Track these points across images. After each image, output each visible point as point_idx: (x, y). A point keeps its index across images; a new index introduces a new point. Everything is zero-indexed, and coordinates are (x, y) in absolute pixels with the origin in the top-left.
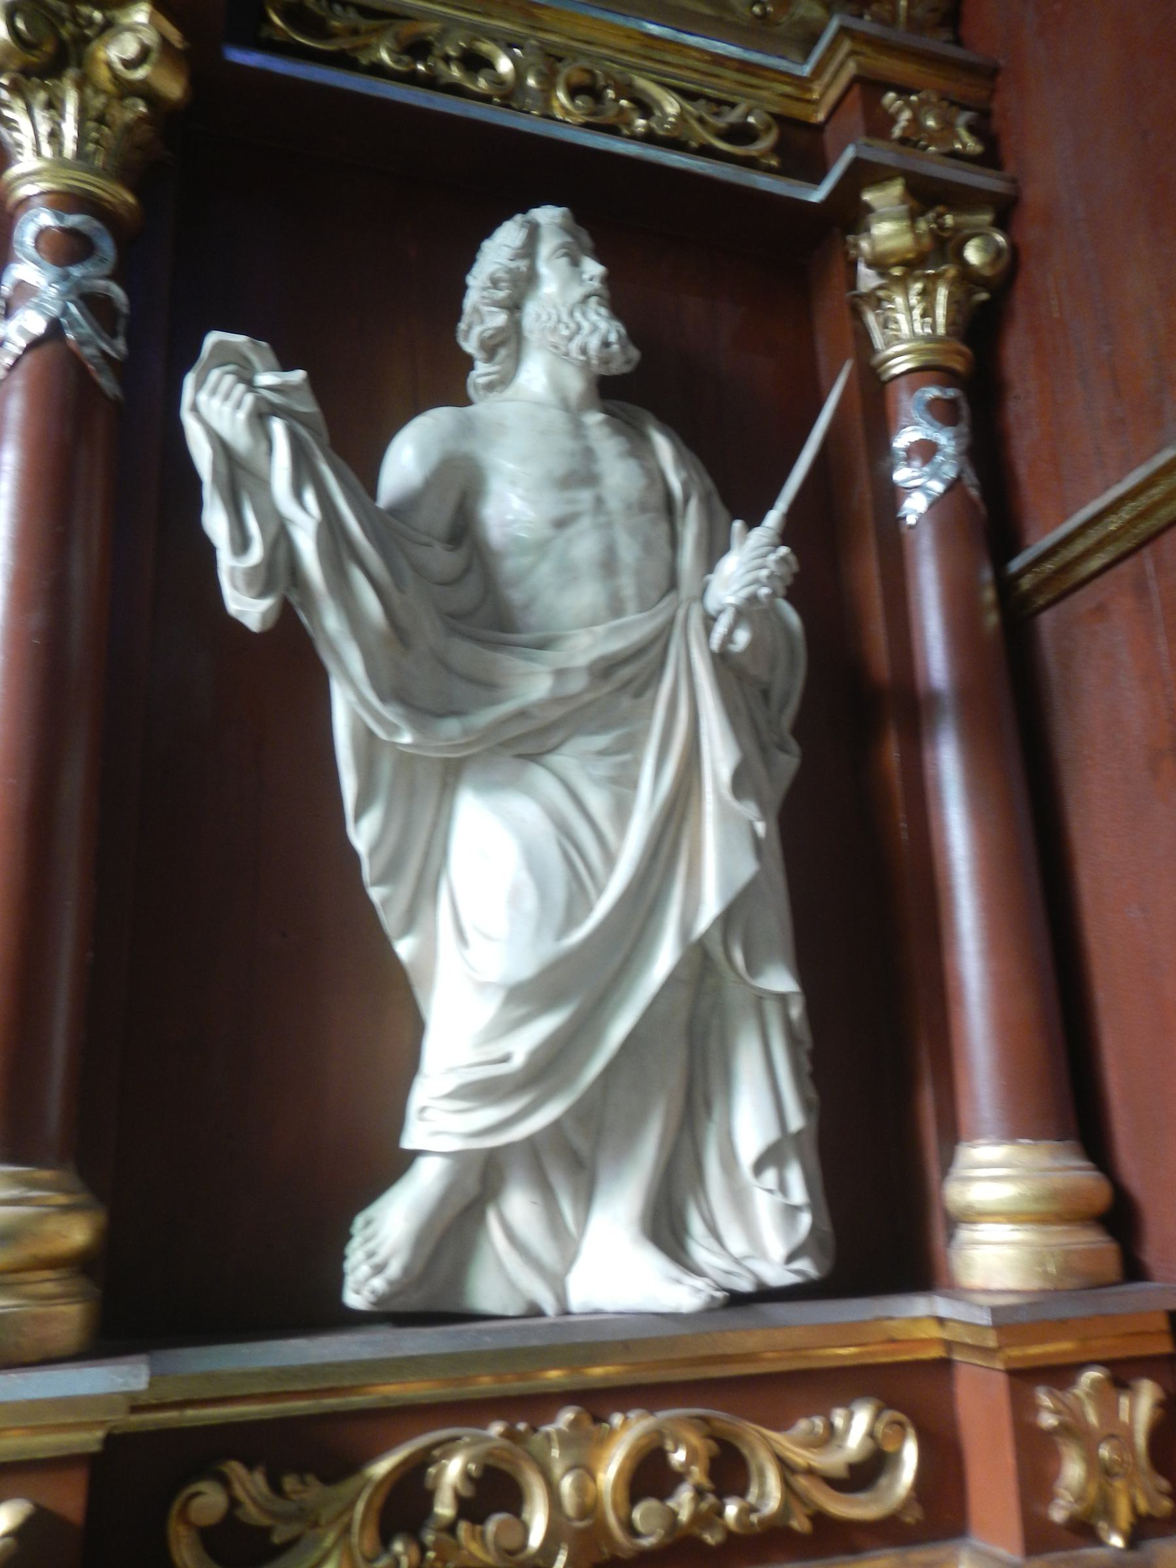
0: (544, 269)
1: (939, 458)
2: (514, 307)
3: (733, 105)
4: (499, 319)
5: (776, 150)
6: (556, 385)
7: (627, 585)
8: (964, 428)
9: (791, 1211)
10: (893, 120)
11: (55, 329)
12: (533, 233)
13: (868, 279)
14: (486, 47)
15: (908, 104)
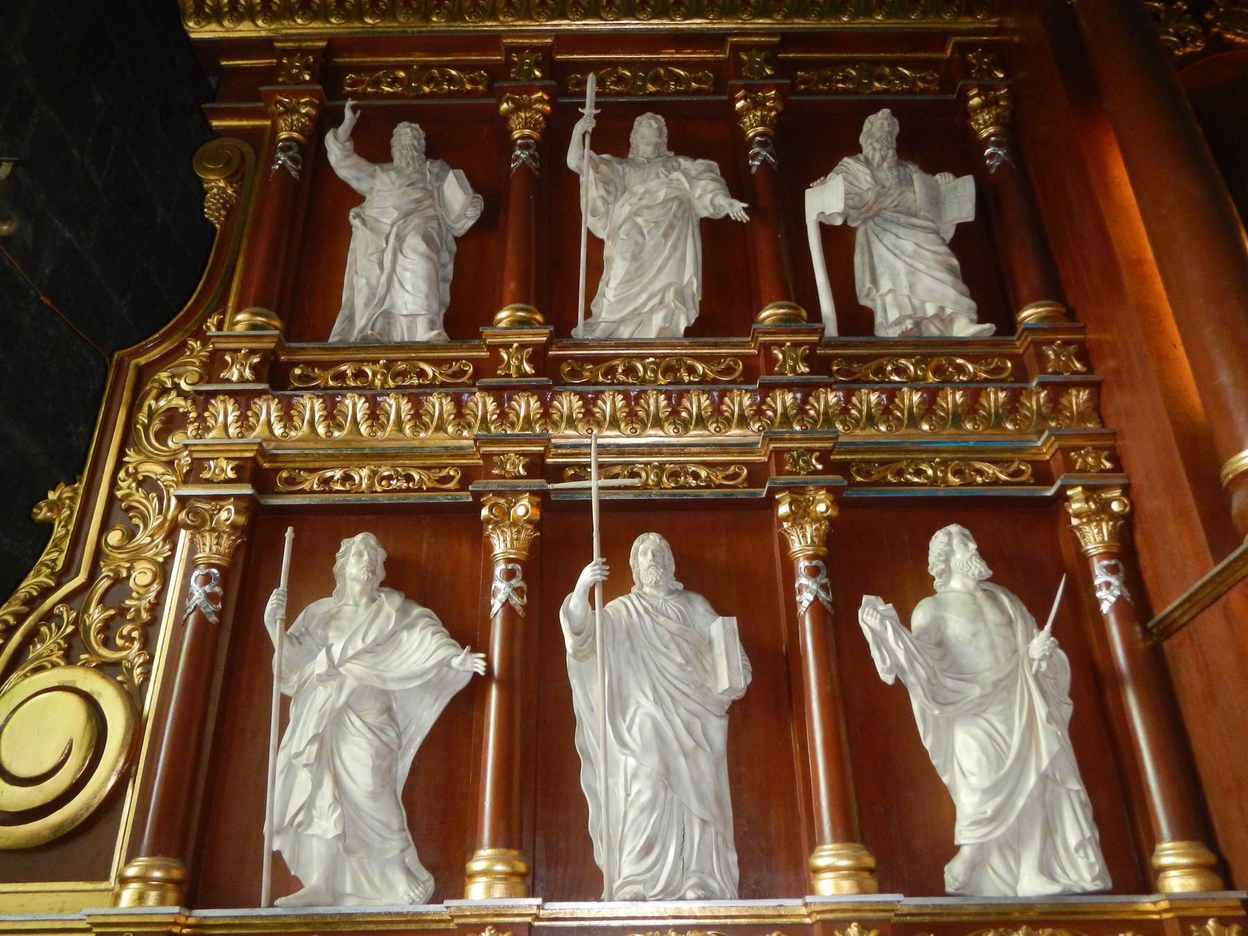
0: (955, 547)
1: (1112, 588)
2: (947, 561)
3: (1013, 462)
4: (943, 566)
5: (1032, 475)
6: (965, 586)
7: (1000, 653)
8: (1121, 574)
9: (1091, 866)
10: (1076, 461)
11: (816, 598)
12: (949, 534)
13: (1075, 521)
14: (923, 467)
15: (1080, 455)
